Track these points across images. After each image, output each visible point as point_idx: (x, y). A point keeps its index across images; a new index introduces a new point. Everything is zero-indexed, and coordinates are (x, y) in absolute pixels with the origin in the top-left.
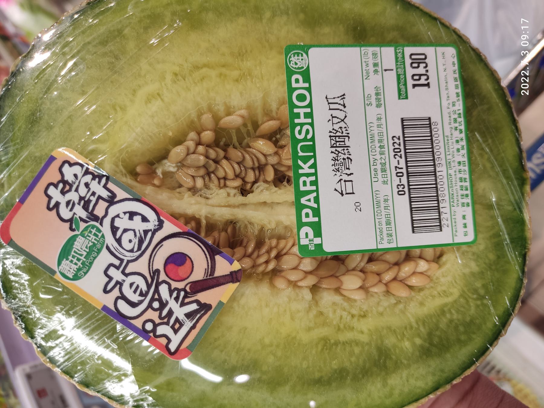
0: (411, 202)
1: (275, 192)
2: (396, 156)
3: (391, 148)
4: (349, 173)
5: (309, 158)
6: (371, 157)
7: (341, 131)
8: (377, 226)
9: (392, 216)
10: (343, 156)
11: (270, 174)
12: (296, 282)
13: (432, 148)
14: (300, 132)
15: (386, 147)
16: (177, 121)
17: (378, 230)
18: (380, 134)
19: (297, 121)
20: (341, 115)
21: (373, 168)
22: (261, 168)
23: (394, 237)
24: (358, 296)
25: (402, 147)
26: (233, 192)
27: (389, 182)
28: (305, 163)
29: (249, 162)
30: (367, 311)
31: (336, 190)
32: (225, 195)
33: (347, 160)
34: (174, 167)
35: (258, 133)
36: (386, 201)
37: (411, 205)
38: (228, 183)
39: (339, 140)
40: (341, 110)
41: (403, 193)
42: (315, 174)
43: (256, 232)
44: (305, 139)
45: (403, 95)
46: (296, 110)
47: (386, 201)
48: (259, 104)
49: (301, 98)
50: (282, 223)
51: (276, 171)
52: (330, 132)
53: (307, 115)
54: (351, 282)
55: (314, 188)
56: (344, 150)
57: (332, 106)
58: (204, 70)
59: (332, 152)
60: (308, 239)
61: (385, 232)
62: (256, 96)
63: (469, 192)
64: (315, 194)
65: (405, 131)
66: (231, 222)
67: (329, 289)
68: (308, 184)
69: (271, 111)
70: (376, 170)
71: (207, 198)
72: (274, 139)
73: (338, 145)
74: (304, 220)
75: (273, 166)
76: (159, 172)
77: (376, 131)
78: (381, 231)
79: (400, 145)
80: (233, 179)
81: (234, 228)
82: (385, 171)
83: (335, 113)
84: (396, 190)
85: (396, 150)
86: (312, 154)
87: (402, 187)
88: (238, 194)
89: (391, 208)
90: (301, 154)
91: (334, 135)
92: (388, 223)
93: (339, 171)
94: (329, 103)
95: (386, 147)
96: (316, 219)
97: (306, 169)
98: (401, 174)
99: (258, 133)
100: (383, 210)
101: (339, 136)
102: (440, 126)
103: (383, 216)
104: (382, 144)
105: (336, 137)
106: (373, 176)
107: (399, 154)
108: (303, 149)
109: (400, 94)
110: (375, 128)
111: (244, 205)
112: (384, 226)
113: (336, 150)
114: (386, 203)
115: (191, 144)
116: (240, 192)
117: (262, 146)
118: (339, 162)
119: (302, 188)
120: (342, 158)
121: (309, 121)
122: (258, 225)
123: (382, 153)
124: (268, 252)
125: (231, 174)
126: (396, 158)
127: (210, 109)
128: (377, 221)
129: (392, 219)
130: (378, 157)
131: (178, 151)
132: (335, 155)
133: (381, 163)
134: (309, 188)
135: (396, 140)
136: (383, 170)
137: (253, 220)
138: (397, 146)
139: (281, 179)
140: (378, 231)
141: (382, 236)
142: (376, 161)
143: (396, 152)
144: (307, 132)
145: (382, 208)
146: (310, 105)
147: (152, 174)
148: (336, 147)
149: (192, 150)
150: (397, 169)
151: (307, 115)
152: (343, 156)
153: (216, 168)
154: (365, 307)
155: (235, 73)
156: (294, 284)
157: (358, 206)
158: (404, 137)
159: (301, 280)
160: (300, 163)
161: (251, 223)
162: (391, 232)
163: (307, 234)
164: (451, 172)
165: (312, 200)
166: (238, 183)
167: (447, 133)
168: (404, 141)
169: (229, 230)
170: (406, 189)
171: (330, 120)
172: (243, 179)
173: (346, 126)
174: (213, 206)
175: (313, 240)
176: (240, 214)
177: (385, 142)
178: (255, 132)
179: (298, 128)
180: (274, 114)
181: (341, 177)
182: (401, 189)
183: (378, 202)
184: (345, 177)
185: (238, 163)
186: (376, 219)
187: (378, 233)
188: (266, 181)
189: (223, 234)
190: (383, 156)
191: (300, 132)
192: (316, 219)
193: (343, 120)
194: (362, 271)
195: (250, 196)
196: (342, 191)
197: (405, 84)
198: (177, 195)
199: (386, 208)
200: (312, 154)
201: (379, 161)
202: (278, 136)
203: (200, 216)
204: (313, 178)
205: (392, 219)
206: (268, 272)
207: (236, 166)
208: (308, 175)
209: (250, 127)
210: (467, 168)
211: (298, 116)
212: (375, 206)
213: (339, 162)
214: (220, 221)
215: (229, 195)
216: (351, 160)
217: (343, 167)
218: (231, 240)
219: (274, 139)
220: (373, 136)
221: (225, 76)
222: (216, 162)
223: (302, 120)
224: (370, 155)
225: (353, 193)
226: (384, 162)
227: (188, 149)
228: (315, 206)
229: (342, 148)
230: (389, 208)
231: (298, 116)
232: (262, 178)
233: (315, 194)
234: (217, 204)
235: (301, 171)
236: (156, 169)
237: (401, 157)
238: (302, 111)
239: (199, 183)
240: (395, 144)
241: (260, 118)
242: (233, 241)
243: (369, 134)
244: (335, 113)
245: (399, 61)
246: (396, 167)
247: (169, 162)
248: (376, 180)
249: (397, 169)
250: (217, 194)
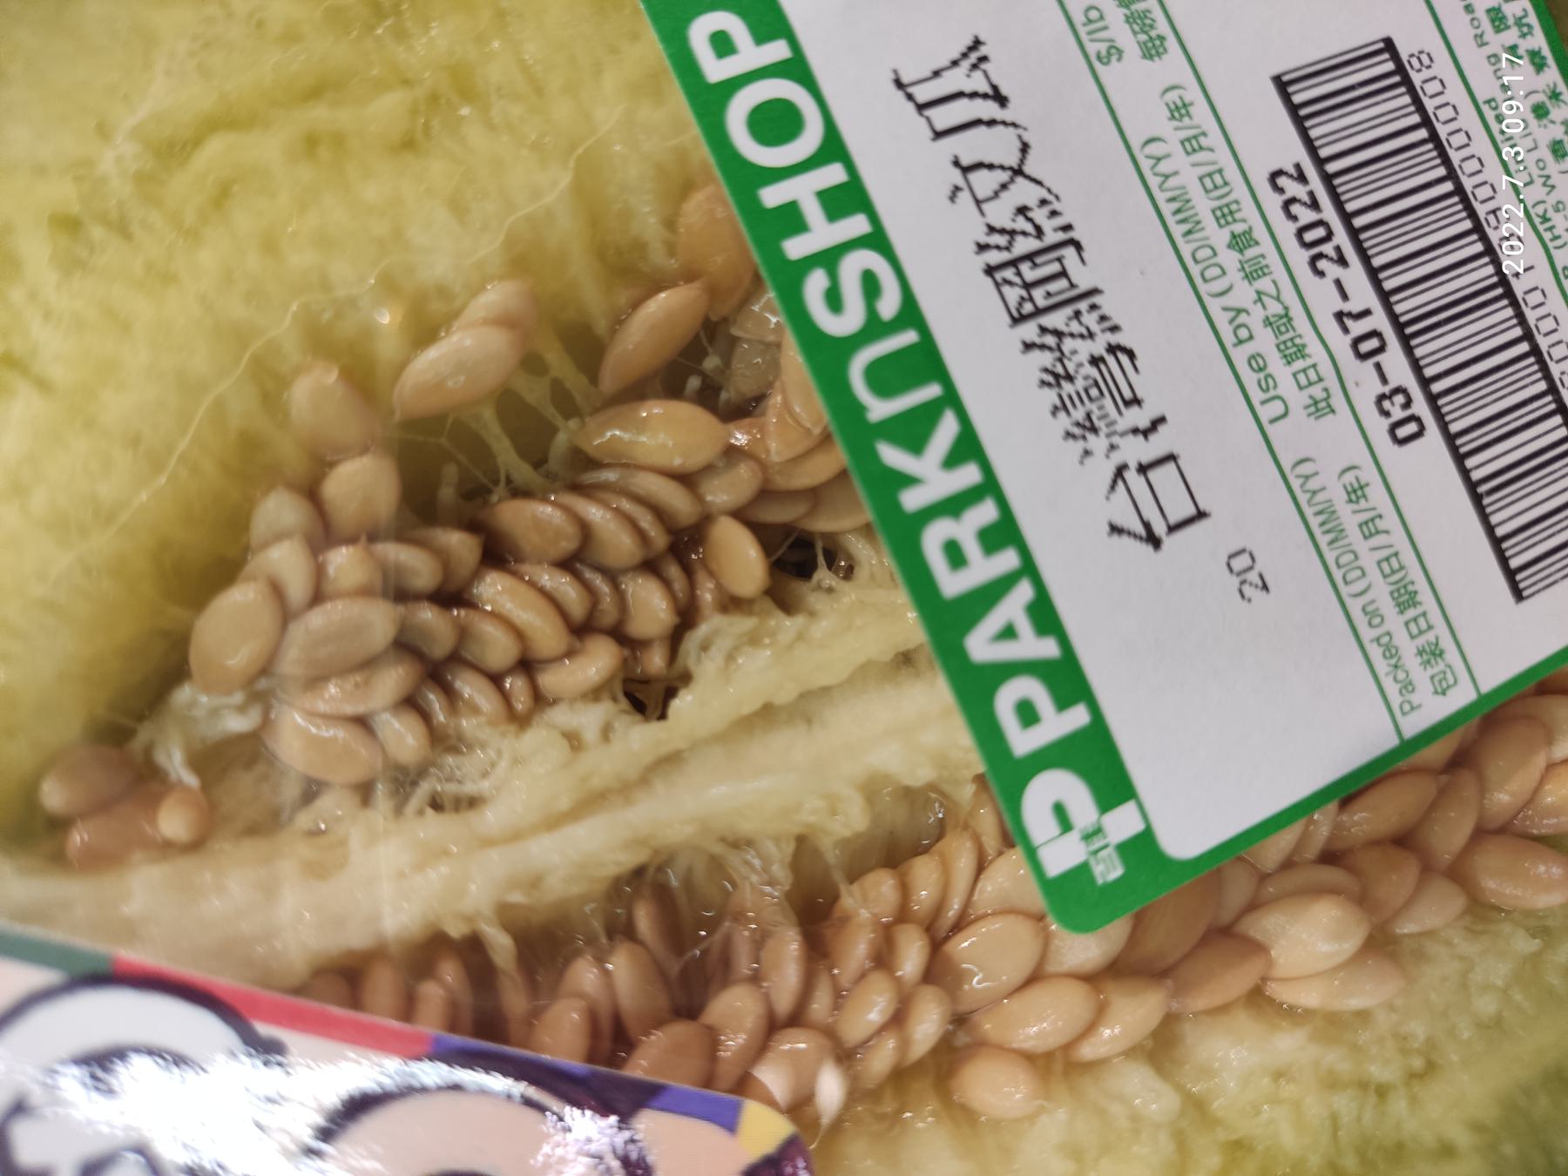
0: (1459, 459)
1: (800, 637)
2: (1322, 264)
3: (1286, 230)
4: (1144, 423)
5: (925, 418)
6: (1214, 306)
7: (1029, 228)
8: (1367, 634)
9: (1408, 557)
10: (1085, 349)
11: (741, 558)
12: (1069, 1047)
13: (1452, 175)
14: (834, 300)
15: (1260, 232)
16: (157, 465)
17: (1375, 652)
18: (1212, 180)
19: (796, 248)
20: (997, 146)
21: (1240, 356)
22: (682, 547)
23: (1452, 655)
24: (1370, 993)
25: (1329, 213)
26: (589, 719)
27: (1338, 400)
29: (618, 543)
30: (1431, 1043)
31: (1115, 530)
32: (558, 750)
33: (1110, 360)
34: (242, 709)
35: (610, 380)
36: (1356, 493)
37: (1465, 473)
38: (550, 680)
39: (1036, 271)
40: (992, 123)
41: (1412, 428)
42: (990, 487)
43: (781, 872)
44: (874, 328)
46: (772, 196)
47: (1356, 493)
48: (567, 231)
50: (886, 778)
51: (764, 534)
52: (982, 248)
54: (1309, 941)
55: (1008, 560)
56: (1077, 314)
57: (945, 116)
58: (216, 148)
59: (1028, 346)
60: (1074, 837)
61: (1408, 649)
62: (541, 189)
64: (1024, 592)
65: (1313, 133)
66: (639, 872)
67: (1223, 1009)
68: (972, 548)
69: (640, 246)
70: (1257, 363)
71: (473, 802)
72: (694, 383)
73: (1041, 302)
74: (1023, 742)
75: (739, 515)
76: (174, 761)
77: (1188, 178)
78: (1390, 651)
79: (1314, 205)
80: (570, 653)
81: (663, 896)
82: (1301, 352)
83: (970, 146)
84: (1378, 427)
85: (1309, 236)
86: (933, 391)
87: (1400, 399)
88: (626, 719)
89: (1390, 521)
90: (879, 409)
91: (1004, 256)
92: (1405, 599)
93: (1094, 430)
94: (921, 108)
95: (1260, 232)
96: (1078, 716)
97: (930, 476)
98: (1373, 343)
99: (610, 380)
100: (1362, 546)
101: (1030, 257)
103: (1374, 575)
104: (1239, 228)
105: (1014, 263)
106: (1256, 396)
107: (1327, 249)
108: (885, 378)
111: (670, 761)
112: (1394, 622)
113: (1043, 330)
114: (1363, 504)
115: (286, 560)
116: (624, 703)
117: (666, 433)
118: (1080, 384)
119: (952, 584)
120: (1083, 357)
122: (777, 840)
123: (1253, 272)
124: (883, 958)
125: (546, 634)
126: (1321, 274)
127: (321, 342)
128: (1355, 606)
129: (1415, 573)
130: (1243, 294)
131: (231, 626)
132: (1047, 359)
133: (1268, 322)
134: (983, 568)
135: (1293, 188)
136: (1293, 352)
137: (747, 827)
138: (1306, 216)
139: (797, 559)
141: (1401, 675)
142: (1243, 318)
143: (1313, 241)
144: (870, 284)
145: (1354, 535)
146: (833, 148)
147: (146, 782)
148: (1039, 312)
149: (297, 586)
150: (1349, 322)
152: (1085, 349)
153: (463, 633)
154: (1418, 1029)
155: (387, 109)
156: (1057, 1066)
157: (1247, 574)
158: (1320, 162)
159: (1090, 1028)
160: (892, 456)
161: (739, 843)
162: (1430, 636)
163: (1060, 811)
165: (1024, 626)
166: (599, 660)
168: (1327, 179)
169: (644, 919)
170: (1421, 407)
171: (957, 189)
172: (619, 634)
173: (1044, 194)
174: (515, 836)
175: (1098, 831)
176: (676, 814)
177: (1248, 211)
178: (594, 379)
179: (816, 284)
180: (658, 257)
181: (1117, 458)
182: (1398, 414)
183: (1328, 512)
184: (1136, 451)
185: (567, 564)
186: (1349, 601)
187: (1382, 666)
188: (732, 604)
189: (622, 965)
190: (1264, 284)
191: (834, 300)
192: (1078, 716)
193: (1018, 172)
194: (1329, 857)
195: (681, 704)
196: (1147, 526)
198: (305, 850)
199: (1369, 528)
200: (933, 391)
201: (1255, 318)
202: (711, 363)
203: (469, 919)
204: (986, 512)
205: (1415, 573)
206: (920, 1064)
207: (564, 586)
208: (954, 506)
209: (559, 363)
211: (791, 219)
212: (1323, 540)
213: (1080, 384)
214: (584, 899)
215: (573, 740)
216: (1131, 355)
217: (1108, 402)
218: (674, 967)
219: (694, 383)
220: (1182, 203)
221: (339, 140)
222: (452, 596)
223: (821, 233)
224: (1207, 300)
225: (1201, 515)
226: (1279, 309)
227: (277, 590)
228: (1048, 648)
229: (1068, 311)
230: (1381, 524)
231: (791, 219)
232: (707, 596)
233: (1024, 592)
234: (541, 810)
235: (912, 500)
236: (148, 751)
237: (1342, 261)
238: (802, 191)
239: (403, 737)
240: (1295, 209)
241: (593, 299)
242: (685, 973)
243: (1161, 198)
244: (970, 146)
246: (1340, 316)
247: (207, 689)
248: (1276, 408)
249: (1349, 322)
250: (516, 761)
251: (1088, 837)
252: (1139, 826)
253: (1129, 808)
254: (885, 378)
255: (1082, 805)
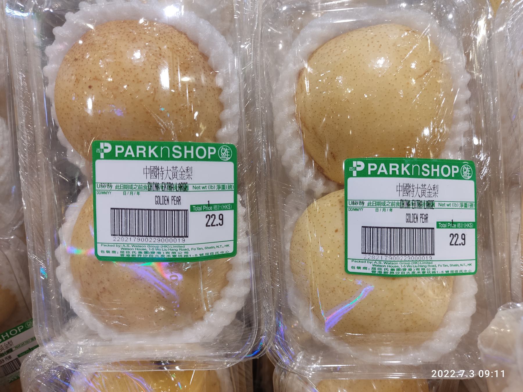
28: (155, 151)
46: (192, 147)
49: (201, 152)
53: (189, 155)
55: (138, 156)
64: (133, 156)
96: (117, 156)
108: (165, 150)
121: (185, 157)
134: (138, 152)
144: (177, 155)
151: (189, 155)
160: (156, 147)
163: (107, 148)
165: (129, 154)
204: (144, 156)
208: (147, 152)
223: (186, 152)
228: (126, 156)
233: (133, 156)
235: (150, 147)
251: (103, 150)
252: (101, 158)
253: (103, 157)
254: (165, 150)
255: (106, 151)
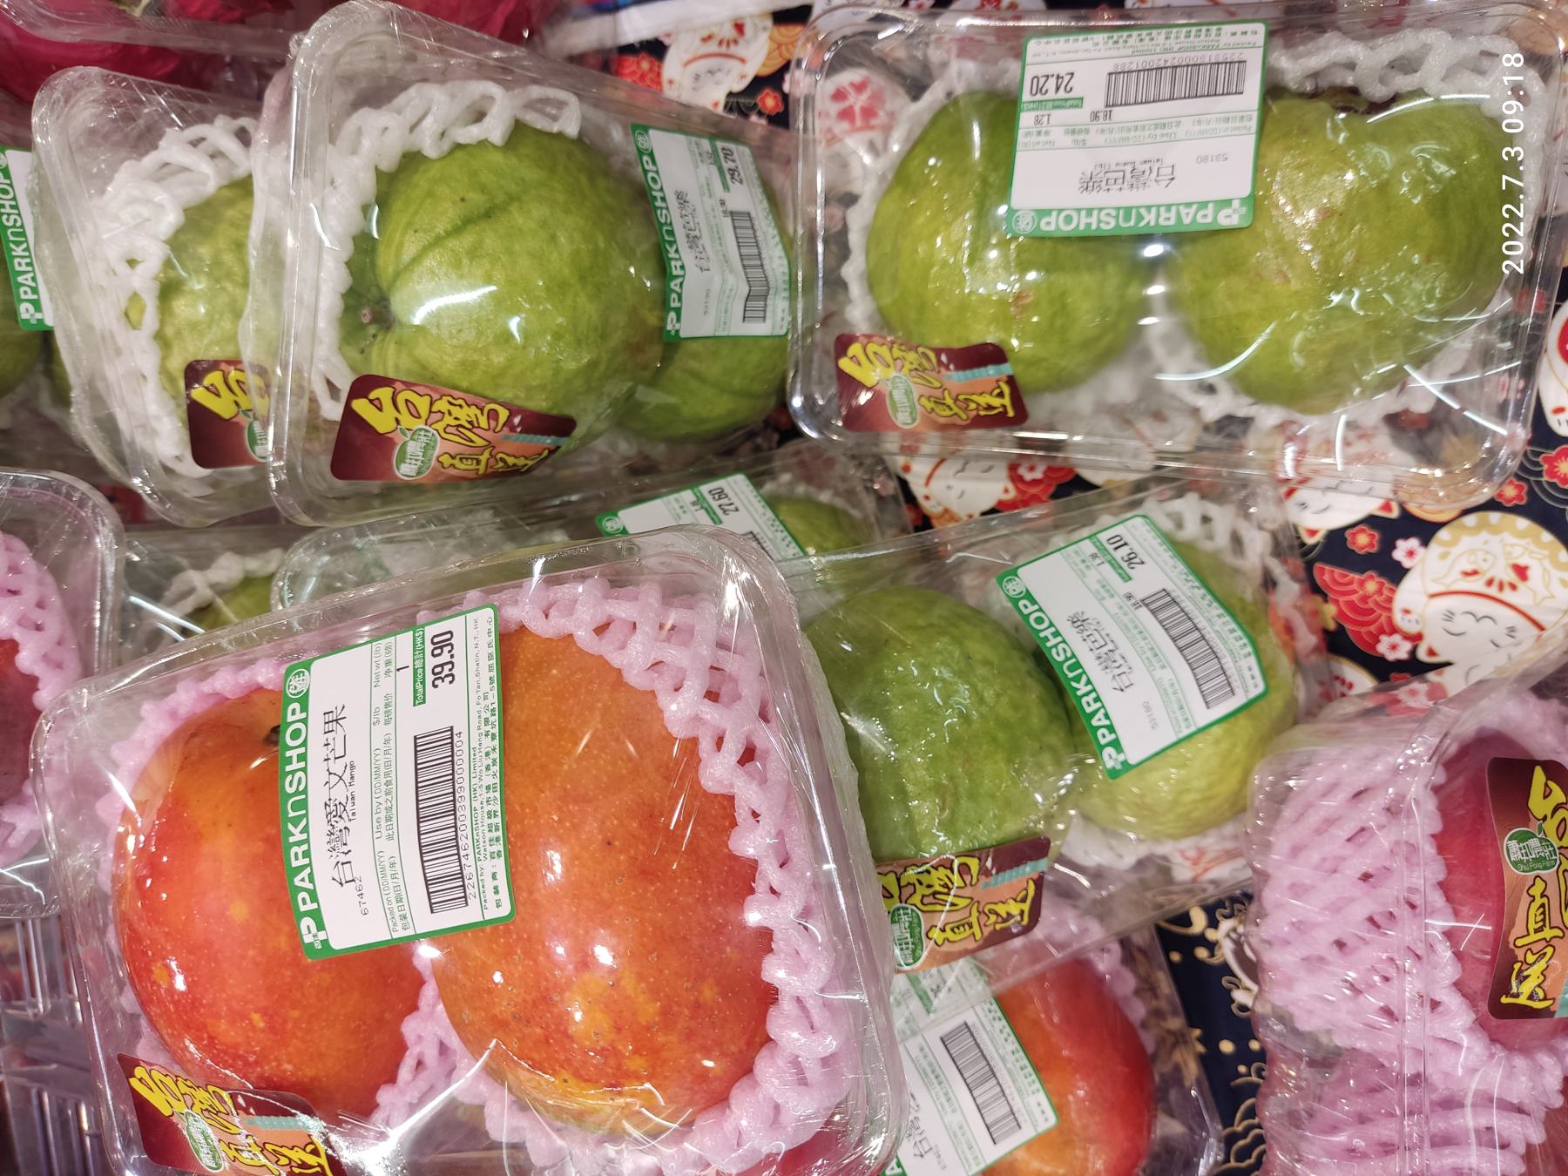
36: (392, 865)
45: (419, 699)
47: (392, 865)
63: (500, 833)
89: (400, 876)
92: (399, 900)
102: (464, 737)
109: (415, 698)
110: (382, 758)
112: (395, 905)
140: (389, 915)
164: (476, 804)
167: (474, 744)
197: (423, 683)
199: (394, 876)
210: (498, 795)
245: (418, 650)
